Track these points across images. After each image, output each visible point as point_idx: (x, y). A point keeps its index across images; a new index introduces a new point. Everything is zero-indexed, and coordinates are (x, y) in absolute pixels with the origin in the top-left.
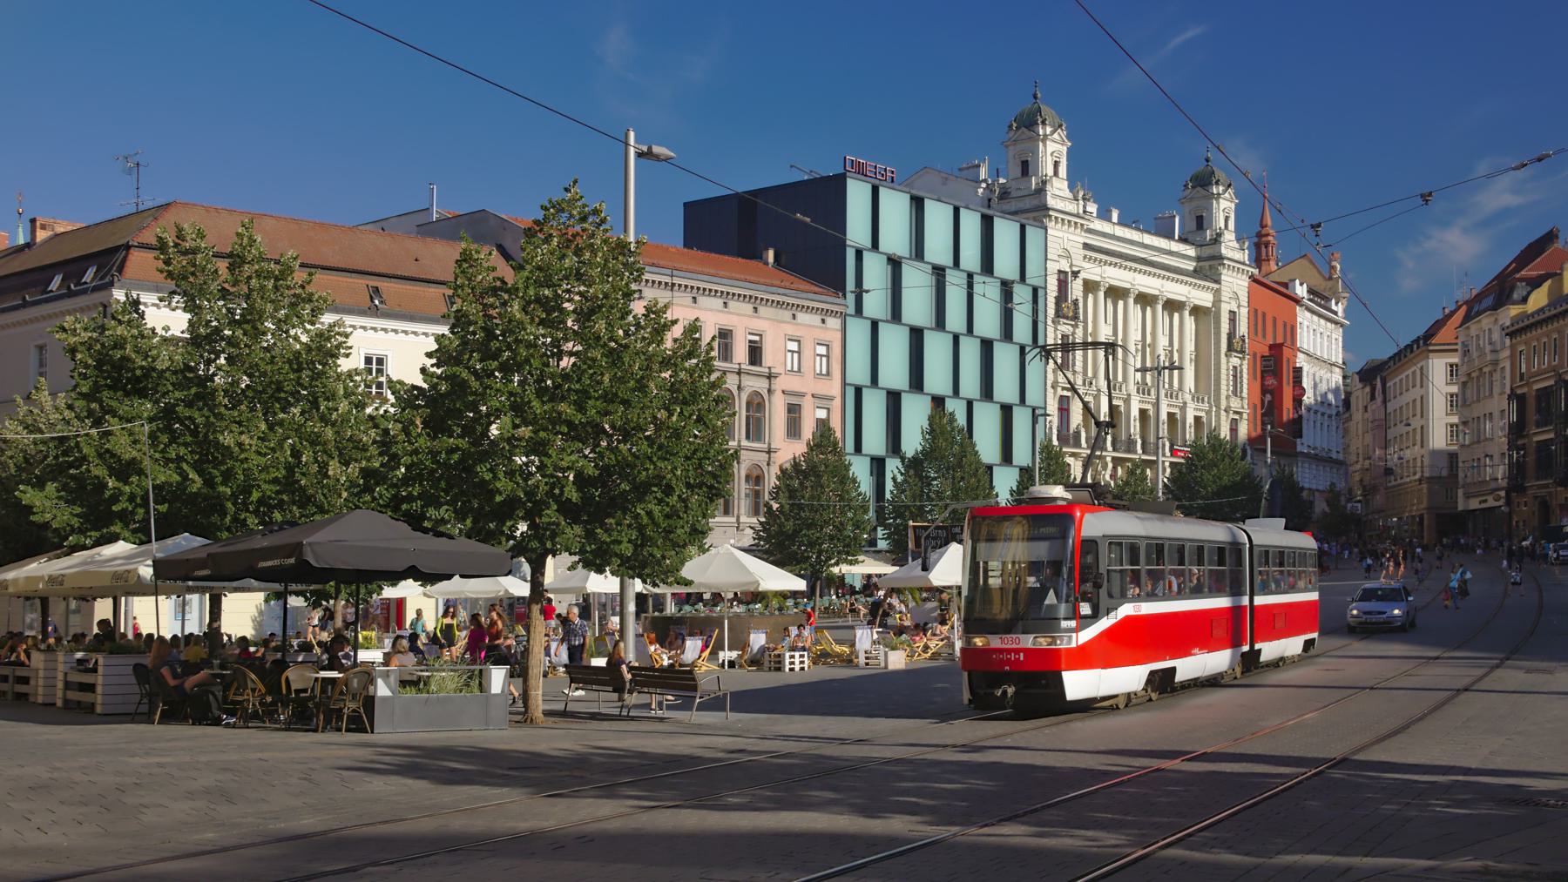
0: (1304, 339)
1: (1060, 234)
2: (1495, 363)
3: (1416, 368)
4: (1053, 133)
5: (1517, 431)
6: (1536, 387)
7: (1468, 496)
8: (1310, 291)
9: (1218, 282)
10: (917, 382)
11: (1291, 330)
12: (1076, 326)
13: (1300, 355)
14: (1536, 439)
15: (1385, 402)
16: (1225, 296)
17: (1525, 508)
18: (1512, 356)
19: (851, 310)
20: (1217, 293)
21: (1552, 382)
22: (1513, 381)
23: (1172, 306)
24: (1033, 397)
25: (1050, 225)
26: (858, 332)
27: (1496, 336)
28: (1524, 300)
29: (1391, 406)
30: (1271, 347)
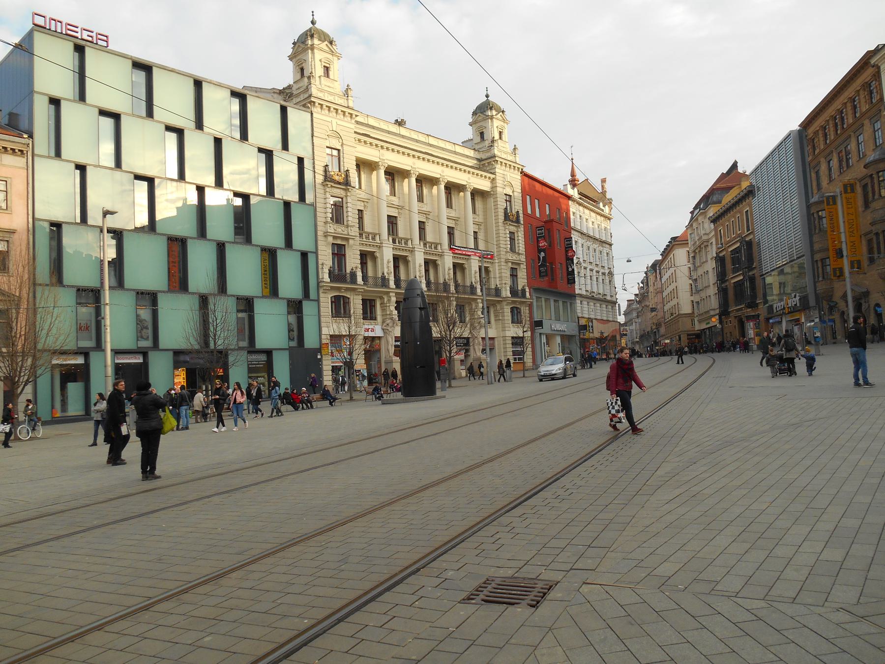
1: (329, 119)
5: (722, 276)
6: (730, 250)
7: (700, 322)
9: (494, 173)
12: (346, 190)
13: (572, 232)
14: (733, 281)
16: (499, 182)
20: (493, 181)
24: (301, 241)
25: (314, 110)
28: (720, 202)
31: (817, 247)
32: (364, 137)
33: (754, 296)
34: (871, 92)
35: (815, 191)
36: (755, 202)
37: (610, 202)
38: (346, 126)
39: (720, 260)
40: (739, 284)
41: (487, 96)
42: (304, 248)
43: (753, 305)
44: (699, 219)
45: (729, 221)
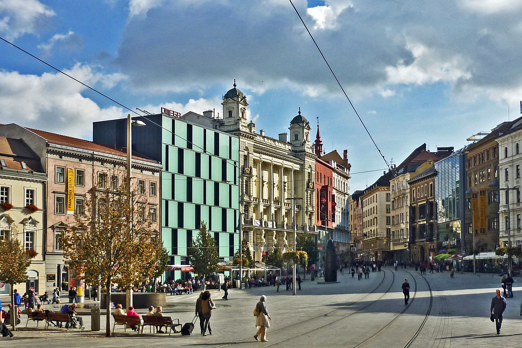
0: (336, 185)
2: (404, 194)
3: (375, 195)
4: (241, 100)
5: (413, 220)
7: (394, 245)
8: (337, 165)
9: (304, 161)
10: (189, 199)
11: (331, 180)
15: (362, 207)
16: (307, 166)
17: (416, 249)
18: (411, 192)
19: (164, 169)
20: (302, 166)
21: (425, 202)
22: (411, 201)
23: (287, 170)
26: (166, 177)
27: (404, 184)
29: (365, 209)
30: (323, 187)
31: (467, 216)
32: (258, 150)
33: (432, 235)
34: (495, 152)
35: (468, 187)
36: (436, 179)
37: (349, 167)
38: (249, 143)
39: (412, 209)
40: (423, 226)
41: (300, 113)
42: (235, 208)
43: (431, 240)
44: (400, 178)
45: (420, 186)
